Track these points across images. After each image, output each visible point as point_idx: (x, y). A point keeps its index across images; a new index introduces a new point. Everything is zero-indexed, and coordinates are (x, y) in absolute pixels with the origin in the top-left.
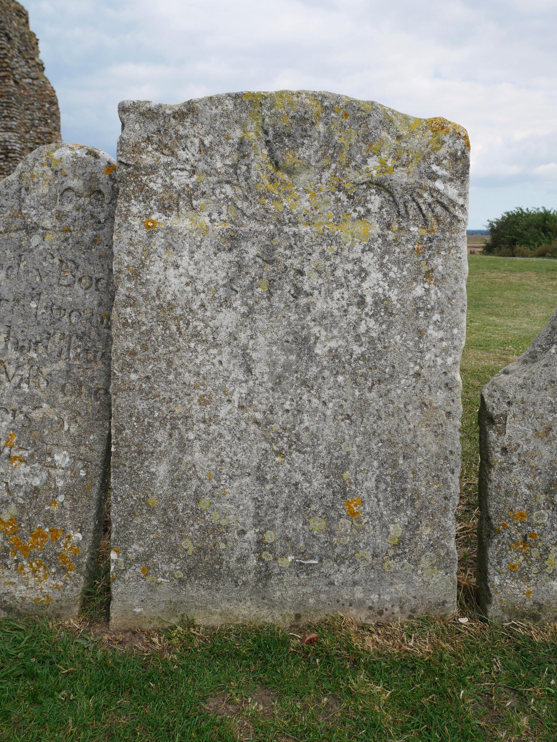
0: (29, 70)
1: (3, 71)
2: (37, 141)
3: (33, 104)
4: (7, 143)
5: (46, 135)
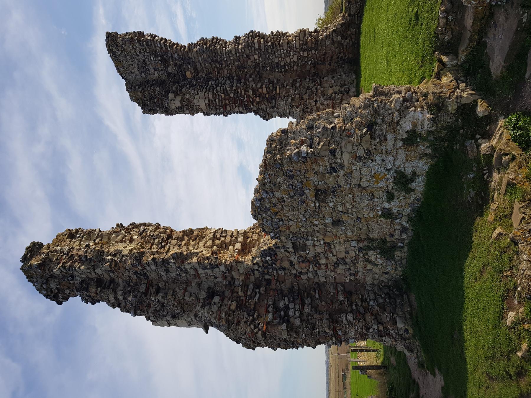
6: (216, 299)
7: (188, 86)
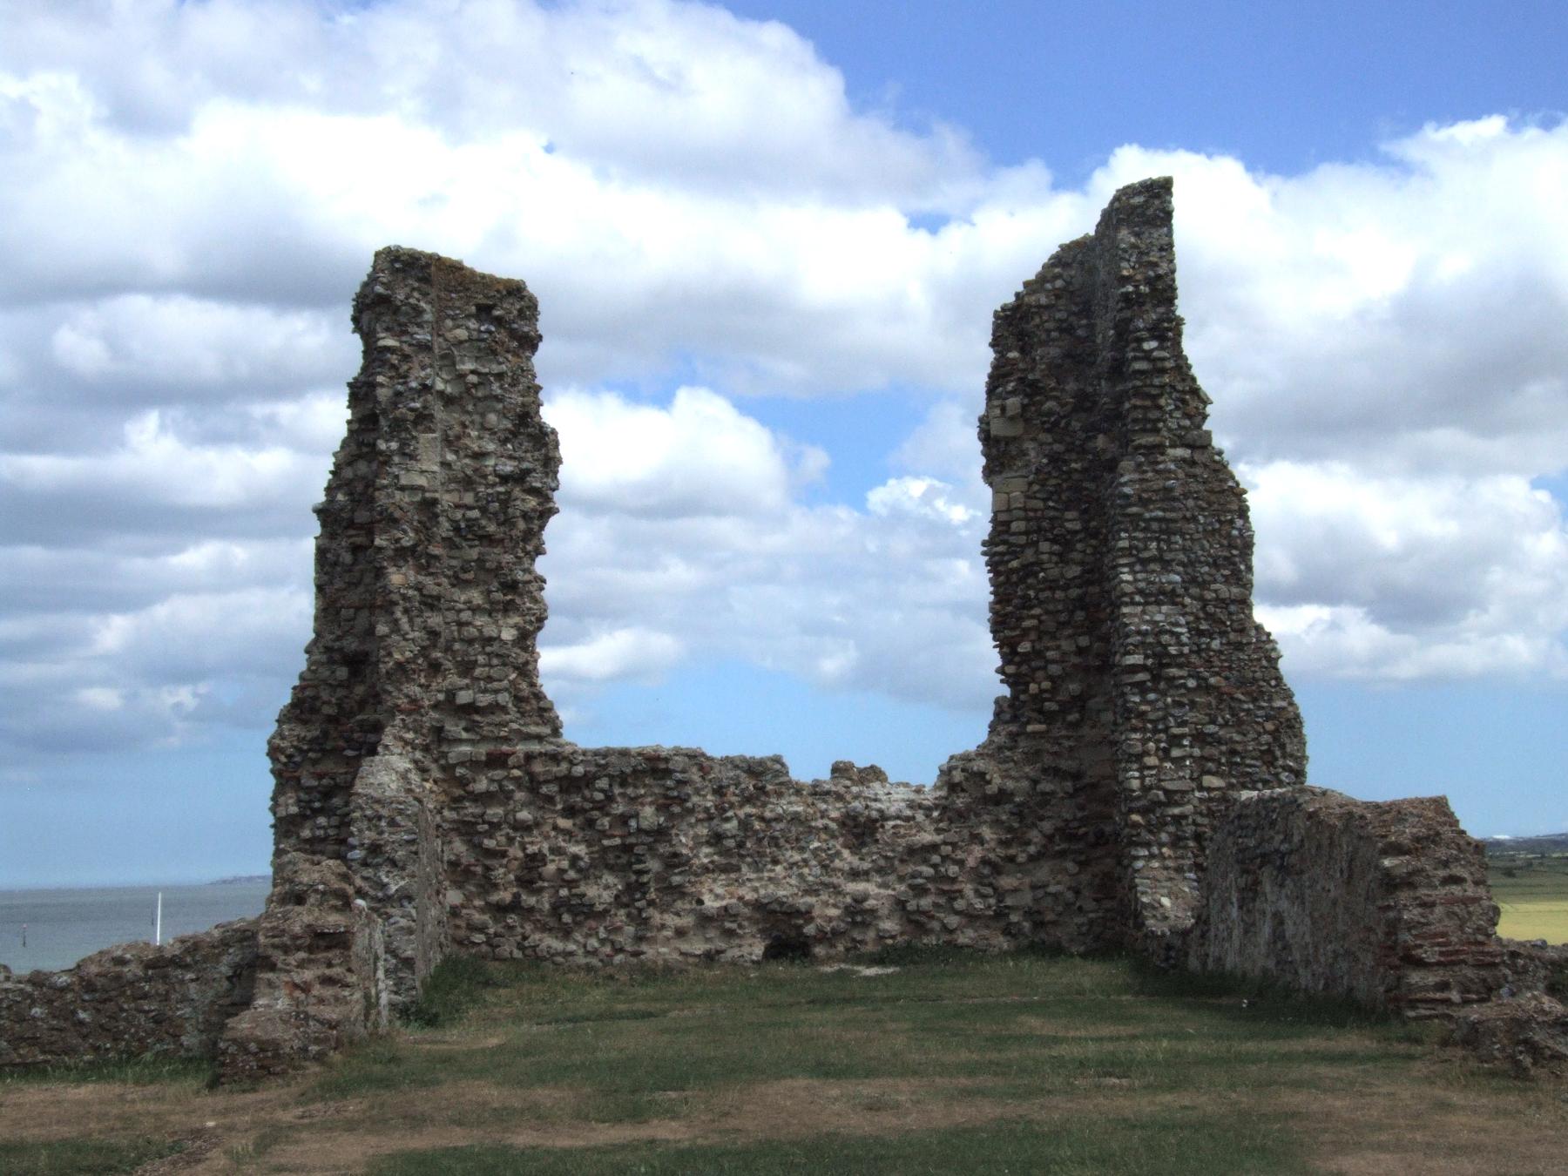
0: (1187, 423)
1: (1144, 431)
2: (1204, 626)
3: (1194, 519)
4: (1165, 638)
5: (1233, 608)
6: (342, 673)
7: (1058, 447)
